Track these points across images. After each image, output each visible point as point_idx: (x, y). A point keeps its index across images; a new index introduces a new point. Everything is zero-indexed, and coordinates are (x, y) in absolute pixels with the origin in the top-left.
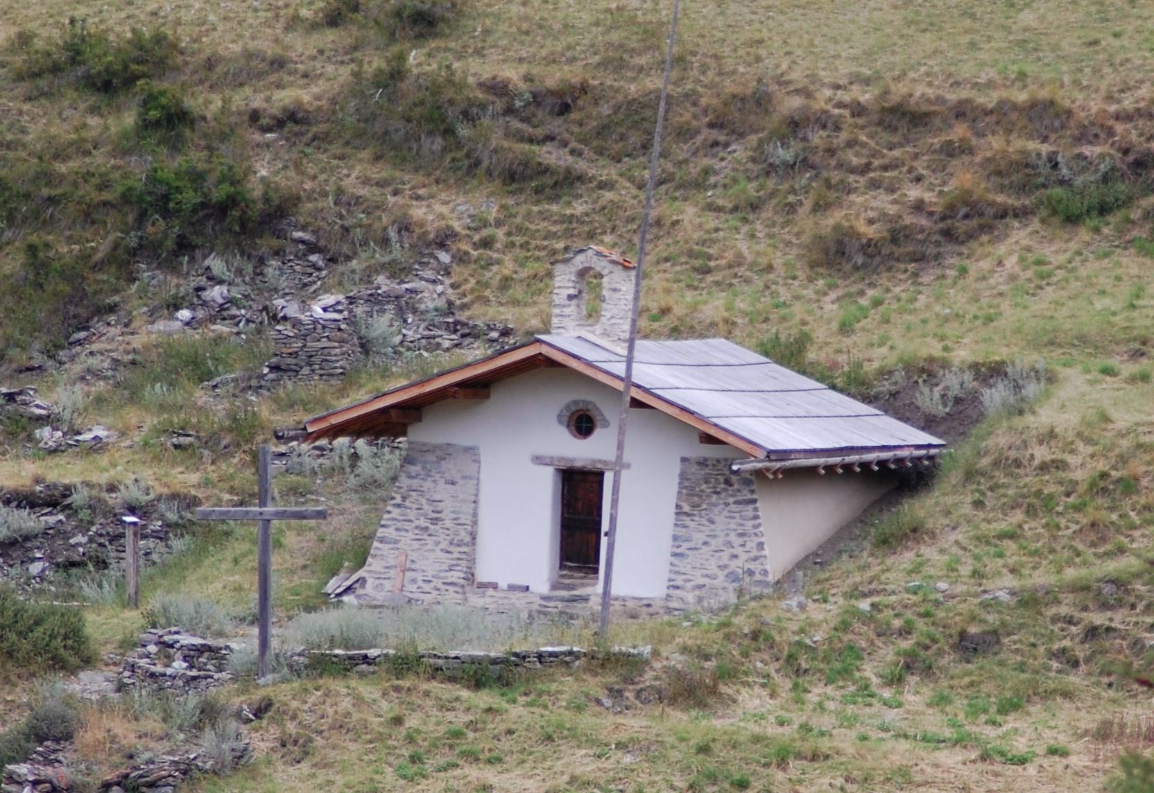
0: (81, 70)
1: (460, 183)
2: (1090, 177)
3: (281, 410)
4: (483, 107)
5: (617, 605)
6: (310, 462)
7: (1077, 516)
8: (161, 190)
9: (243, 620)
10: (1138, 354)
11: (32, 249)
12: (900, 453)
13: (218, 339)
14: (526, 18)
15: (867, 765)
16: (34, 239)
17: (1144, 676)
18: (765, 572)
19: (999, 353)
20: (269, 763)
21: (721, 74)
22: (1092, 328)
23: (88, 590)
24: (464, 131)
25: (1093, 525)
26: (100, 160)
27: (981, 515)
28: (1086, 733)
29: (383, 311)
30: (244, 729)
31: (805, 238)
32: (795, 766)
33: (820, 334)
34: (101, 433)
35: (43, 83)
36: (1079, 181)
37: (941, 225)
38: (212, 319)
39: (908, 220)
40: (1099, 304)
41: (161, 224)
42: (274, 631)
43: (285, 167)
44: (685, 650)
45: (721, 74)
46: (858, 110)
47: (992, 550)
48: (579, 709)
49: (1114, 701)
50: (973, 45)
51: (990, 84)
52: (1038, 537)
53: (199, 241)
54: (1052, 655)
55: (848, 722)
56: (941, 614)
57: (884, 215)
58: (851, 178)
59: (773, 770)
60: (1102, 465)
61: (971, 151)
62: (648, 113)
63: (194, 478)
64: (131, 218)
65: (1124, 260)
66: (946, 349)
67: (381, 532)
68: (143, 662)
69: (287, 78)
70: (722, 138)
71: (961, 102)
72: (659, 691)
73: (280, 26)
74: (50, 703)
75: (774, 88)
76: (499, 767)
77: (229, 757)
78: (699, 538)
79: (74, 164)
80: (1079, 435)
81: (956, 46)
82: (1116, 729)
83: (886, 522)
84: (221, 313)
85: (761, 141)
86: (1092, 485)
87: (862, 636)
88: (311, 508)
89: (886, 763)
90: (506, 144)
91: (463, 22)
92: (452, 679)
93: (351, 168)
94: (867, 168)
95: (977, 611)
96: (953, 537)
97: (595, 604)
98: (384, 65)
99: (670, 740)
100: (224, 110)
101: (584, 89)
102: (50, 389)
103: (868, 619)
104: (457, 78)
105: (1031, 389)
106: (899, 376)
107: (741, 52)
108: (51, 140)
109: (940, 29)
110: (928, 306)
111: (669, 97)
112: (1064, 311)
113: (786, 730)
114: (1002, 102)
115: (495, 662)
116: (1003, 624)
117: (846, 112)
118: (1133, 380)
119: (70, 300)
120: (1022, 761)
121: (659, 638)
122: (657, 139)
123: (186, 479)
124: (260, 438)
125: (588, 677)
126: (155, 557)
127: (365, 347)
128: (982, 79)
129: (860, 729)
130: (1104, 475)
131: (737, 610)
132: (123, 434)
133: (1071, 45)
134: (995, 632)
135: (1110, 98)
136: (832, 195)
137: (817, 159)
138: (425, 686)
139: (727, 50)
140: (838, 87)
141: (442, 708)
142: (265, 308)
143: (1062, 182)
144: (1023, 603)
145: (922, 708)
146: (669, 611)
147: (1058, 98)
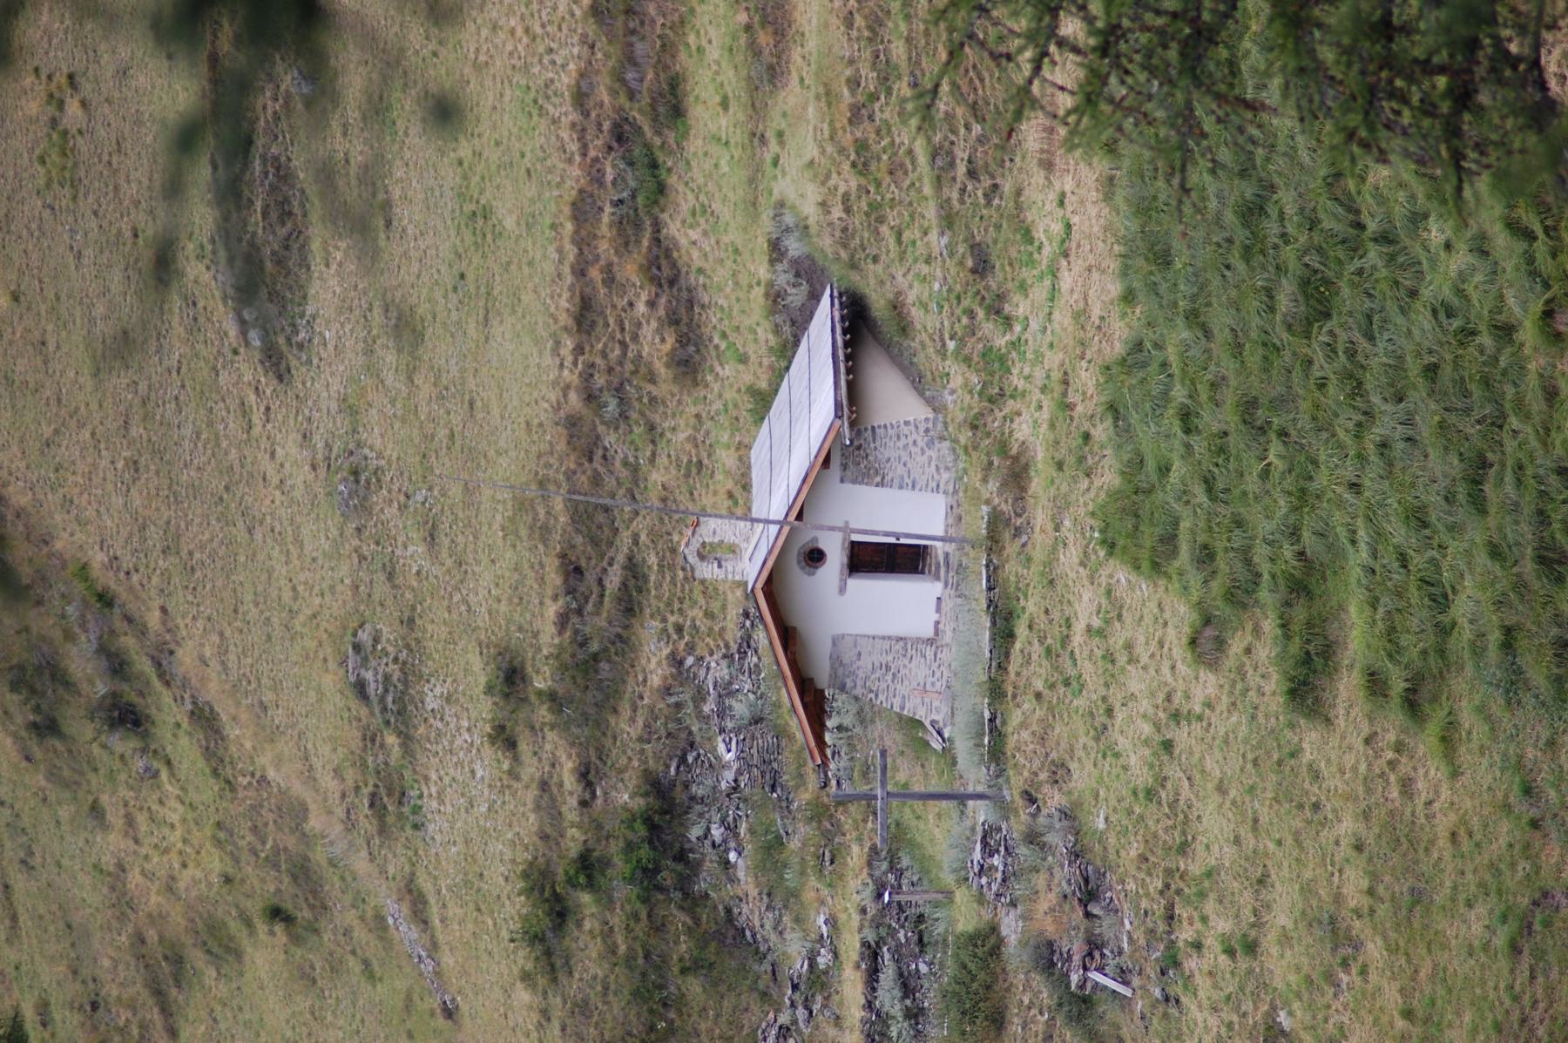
0: (549, 934)
1: (634, 649)
2: (629, 176)
3: (804, 784)
4: (576, 632)
5: (951, 531)
6: (844, 762)
7: (884, 185)
8: (639, 874)
9: (962, 813)
10: (763, 140)
11: (684, 971)
12: (837, 318)
13: (751, 831)
14: (510, 599)
15: (1071, 343)
16: (676, 970)
17: (1004, 135)
18: (927, 420)
19: (762, 244)
20: (1070, 792)
21: (552, 453)
22: (743, 174)
23: (940, 928)
24: (595, 646)
25: (891, 173)
26: (617, 920)
27: (883, 257)
28: (1047, 178)
29: (730, 707)
30: (1045, 811)
31: (675, 390)
32: (1072, 397)
33: (748, 378)
34: (821, 919)
35: (559, 963)
36: (632, 184)
37: (666, 287)
38: (736, 835)
39: (662, 312)
40: (725, 168)
41: (664, 874)
42: (970, 789)
43: (622, 780)
44: (985, 480)
45: (552, 453)
46: (579, 350)
47: (910, 249)
48: (1029, 560)
49: (1024, 158)
50: (530, 264)
51: (560, 251)
52: (900, 214)
53: (677, 846)
54: (989, 203)
55: (1039, 358)
56: (958, 288)
57: (658, 331)
58: (630, 355)
59: (1075, 414)
60: (846, 166)
61: (610, 265)
62: (581, 508)
63: (855, 849)
64: (660, 897)
65: (692, 149)
66: (759, 284)
67: (897, 709)
68: (994, 887)
69: (555, 779)
70: (600, 452)
71: (573, 272)
72: (1016, 500)
73: (515, 785)
74: (1025, 958)
75: (562, 414)
76: (1073, 620)
77: (1066, 823)
78: (901, 470)
79: (620, 939)
80: (823, 183)
81: (531, 276)
82: (1044, 156)
83: (889, 329)
84: (731, 829)
85: (603, 423)
86: (860, 173)
87: (975, 347)
88: (878, 761)
89: (1070, 329)
90: (605, 615)
91: (512, 647)
92: (1007, 655)
93: (622, 731)
94: (623, 344)
95: (955, 260)
96: (900, 279)
97: (950, 548)
98: (545, 707)
99: (1052, 491)
100: (579, 826)
101: (563, 556)
102: (789, 957)
103: (962, 342)
104: (555, 651)
105: (789, 219)
106: (779, 319)
107: (535, 437)
108: (601, 957)
109: (518, 288)
110: (727, 297)
111: (569, 492)
112: (730, 195)
113: (1045, 404)
114: (573, 242)
115: (994, 623)
116: (965, 241)
117: (581, 359)
118: (782, 143)
119: (722, 942)
120: (1069, 226)
121: (976, 499)
122: (601, 501)
123: (856, 855)
124: (826, 800)
125: (1005, 554)
126: (915, 879)
127: (757, 720)
128: (556, 256)
129: (1045, 349)
130: (854, 165)
131: (955, 441)
132: (823, 903)
133: (530, 190)
134: (972, 247)
135: (570, 161)
136: (643, 370)
137: (616, 381)
138: (1012, 675)
139: (534, 449)
140: (562, 365)
141: (1028, 663)
142: (728, 795)
143: (633, 197)
144: (950, 226)
145: (1028, 302)
146: (955, 492)
147: (570, 199)
